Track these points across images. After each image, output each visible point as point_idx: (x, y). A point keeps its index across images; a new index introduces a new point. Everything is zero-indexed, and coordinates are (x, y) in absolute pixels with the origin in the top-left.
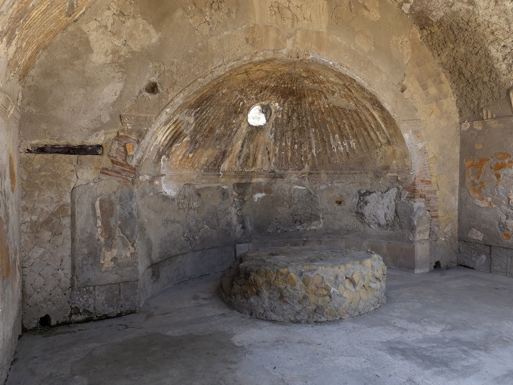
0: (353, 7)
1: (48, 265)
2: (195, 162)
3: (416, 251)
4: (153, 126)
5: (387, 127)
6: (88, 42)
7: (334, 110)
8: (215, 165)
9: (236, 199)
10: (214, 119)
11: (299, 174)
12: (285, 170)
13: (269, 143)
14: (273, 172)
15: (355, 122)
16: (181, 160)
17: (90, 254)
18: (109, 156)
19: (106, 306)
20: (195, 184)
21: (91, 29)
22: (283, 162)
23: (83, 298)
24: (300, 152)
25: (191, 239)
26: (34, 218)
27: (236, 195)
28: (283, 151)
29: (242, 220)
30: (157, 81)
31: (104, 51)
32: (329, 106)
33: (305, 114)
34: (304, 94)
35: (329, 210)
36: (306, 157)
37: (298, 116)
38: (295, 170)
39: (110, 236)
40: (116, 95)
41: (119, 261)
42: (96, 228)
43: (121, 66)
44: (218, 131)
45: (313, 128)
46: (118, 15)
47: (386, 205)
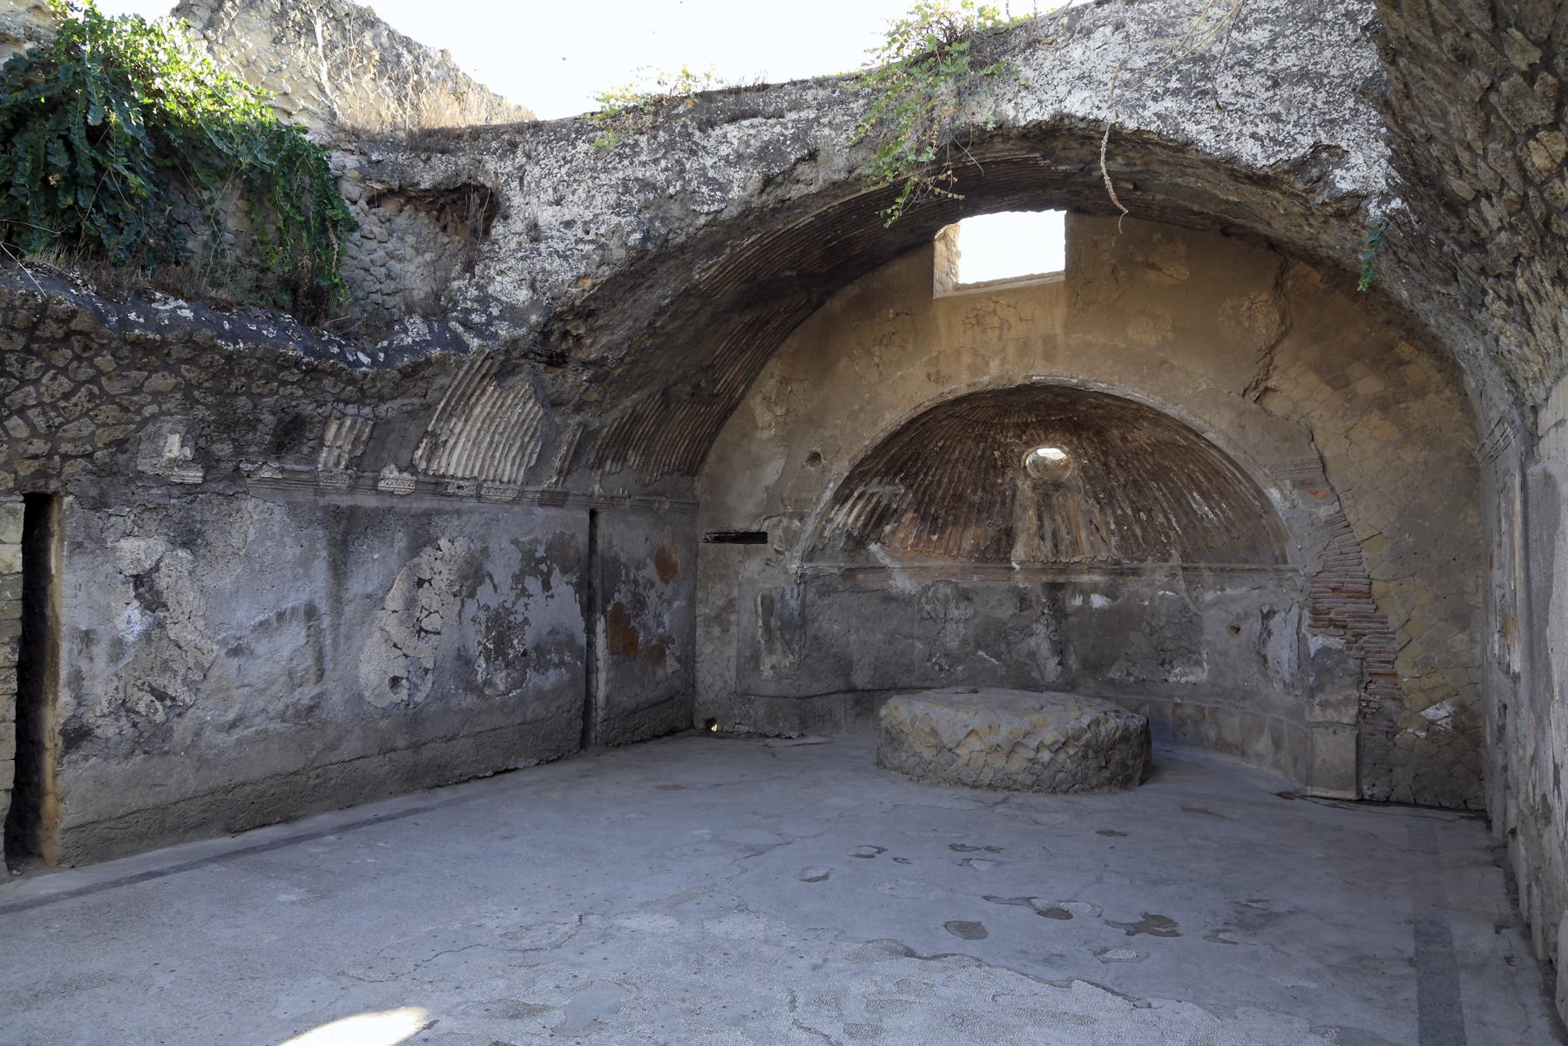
8: (997, 551)
10: (950, 481)
14: (1118, 562)
17: (752, 657)
36: (1168, 536)
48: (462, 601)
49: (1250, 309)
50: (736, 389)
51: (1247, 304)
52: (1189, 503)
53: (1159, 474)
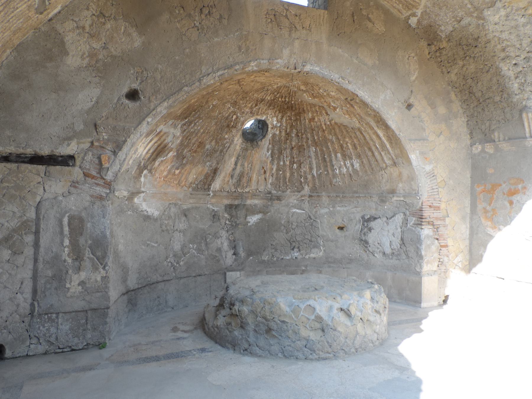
1: (5, 287)
2: (183, 179)
3: (423, 283)
4: (132, 136)
5: (392, 147)
6: (63, 43)
7: (336, 127)
8: (205, 184)
9: (227, 222)
10: (204, 132)
11: (298, 197)
12: (283, 192)
13: (266, 162)
15: (359, 140)
16: (166, 177)
17: (54, 277)
18: (80, 167)
19: (70, 336)
20: (181, 203)
21: (67, 30)
22: (281, 183)
23: (44, 327)
24: (300, 172)
25: (175, 264)
27: (228, 218)
28: (281, 171)
29: (233, 246)
30: (139, 88)
31: (81, 53)
32: (331, 123)
34: (303, 109)
35: (330, 236)
36: (306, 178)
37: (297, 133)
38: (294, 192)
39: (78, 256)
40: (92, 101)
41: (87, 285)
42: (63, 248)
44: (208, 146)
45: (314, 146)
46: (98, 17)
47: (391, 232)
52: (331, 161)
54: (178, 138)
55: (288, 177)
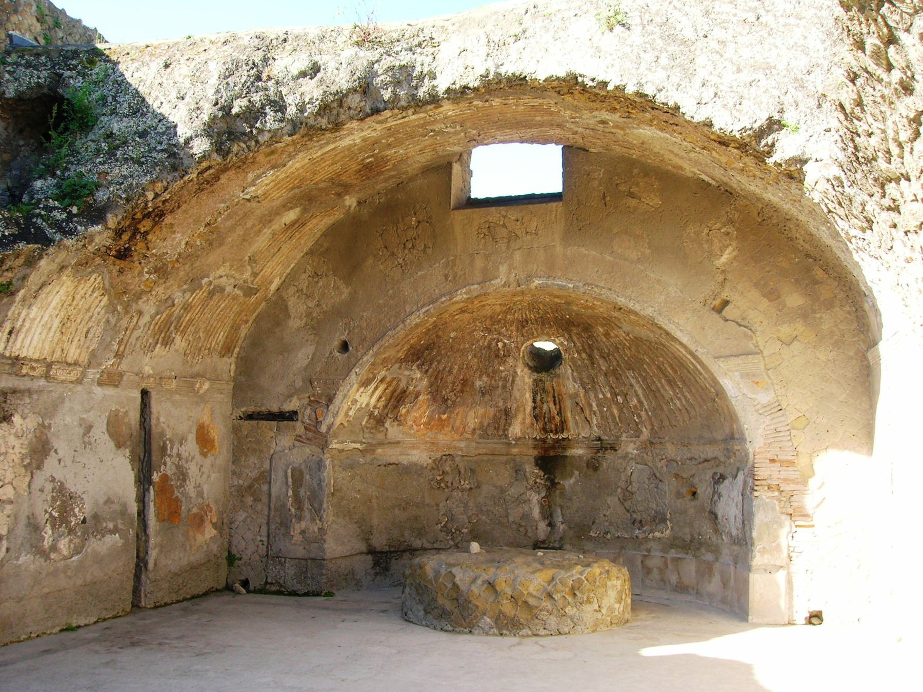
0: (608, 199)
1: (249, 529)
4: (341, 388)
6: (286, 307)
10: (460, 369)
18: (303, 422)
26: (241, 482)
33: (609, 350)
43: (313, 328)
44: (478, 384)
48: (32, 474)
49: (708, 235)
50: (271, 282)
51: (706, 231)
53: (635, 365)
54: (421, 379)
55: (617, 416)
